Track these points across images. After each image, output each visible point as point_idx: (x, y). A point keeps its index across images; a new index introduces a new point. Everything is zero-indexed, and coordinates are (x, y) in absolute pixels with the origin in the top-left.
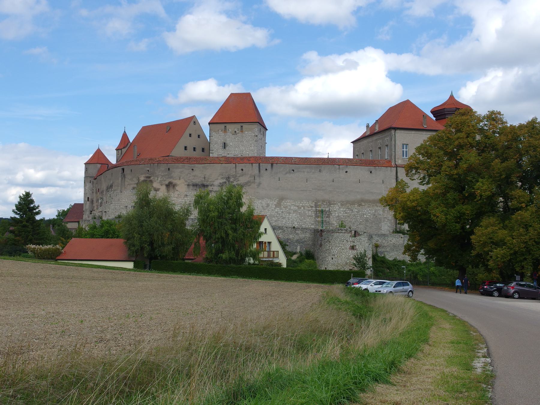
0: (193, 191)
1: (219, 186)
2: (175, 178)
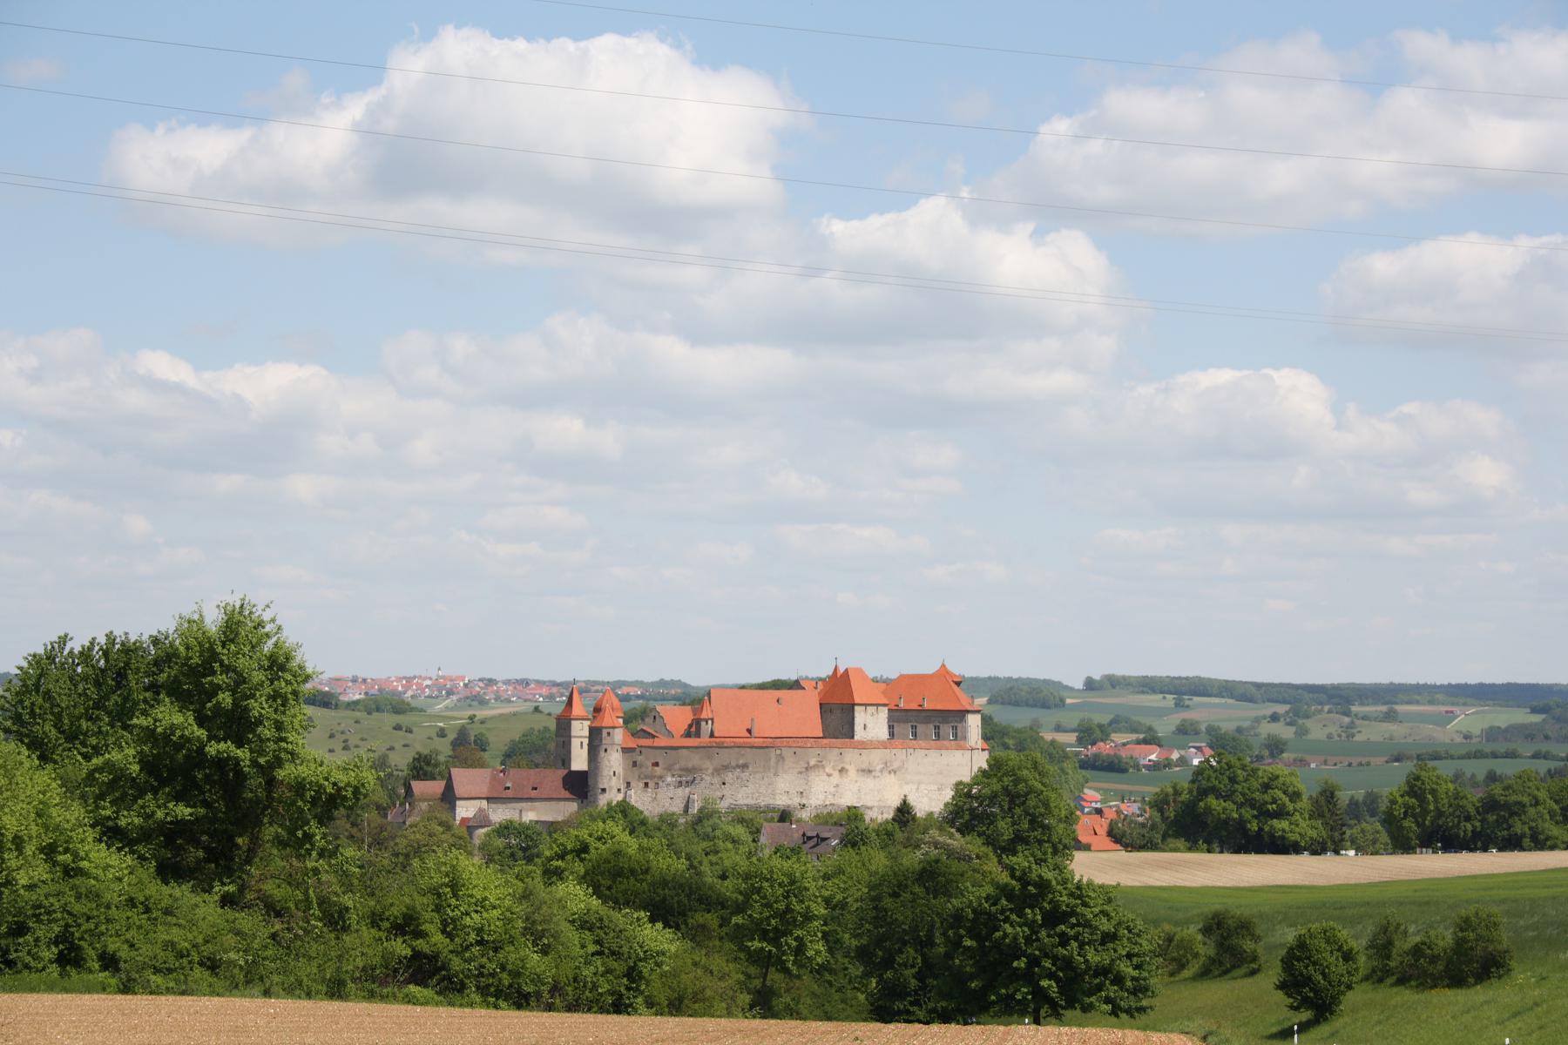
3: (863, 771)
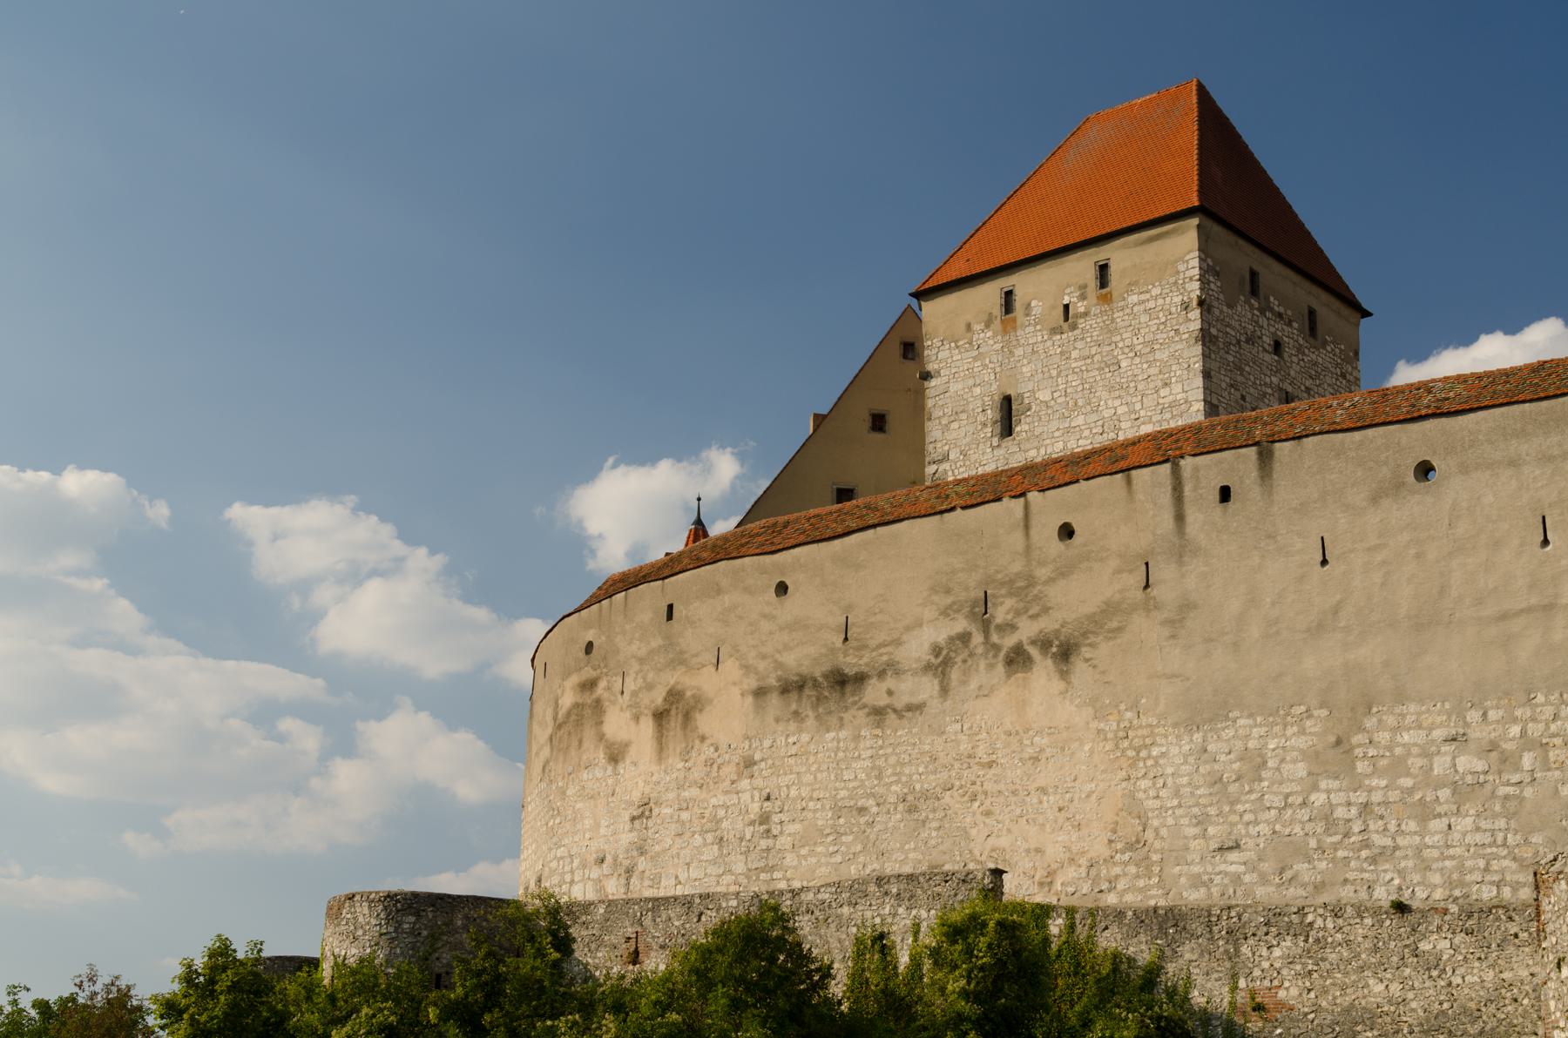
1: (928, 667)
2: (694, 661)
3: (793, 687)
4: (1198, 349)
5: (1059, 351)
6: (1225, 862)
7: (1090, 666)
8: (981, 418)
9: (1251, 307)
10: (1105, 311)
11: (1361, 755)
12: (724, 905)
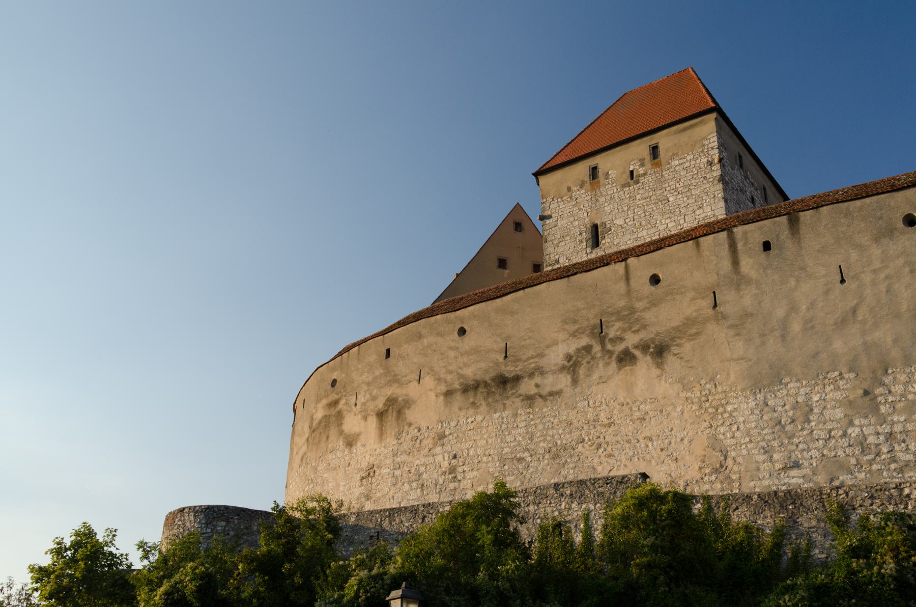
0: (462, 413)
1: (563, 368)
3: (471, 388)
4: (720, 186)
5: (628, 197)
6: (788, 477)
7: (678, 358)
8: (579, 238)
9: (741, 173)
10: (657, 171)
11: (883, 401)
12: (441, 510)
